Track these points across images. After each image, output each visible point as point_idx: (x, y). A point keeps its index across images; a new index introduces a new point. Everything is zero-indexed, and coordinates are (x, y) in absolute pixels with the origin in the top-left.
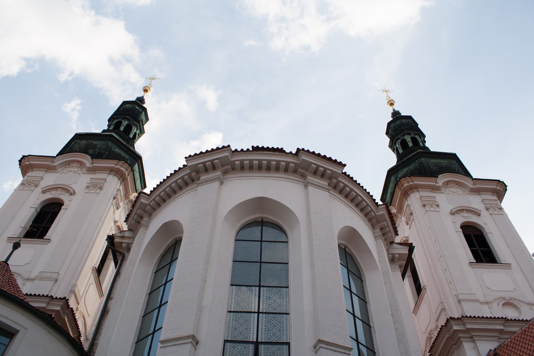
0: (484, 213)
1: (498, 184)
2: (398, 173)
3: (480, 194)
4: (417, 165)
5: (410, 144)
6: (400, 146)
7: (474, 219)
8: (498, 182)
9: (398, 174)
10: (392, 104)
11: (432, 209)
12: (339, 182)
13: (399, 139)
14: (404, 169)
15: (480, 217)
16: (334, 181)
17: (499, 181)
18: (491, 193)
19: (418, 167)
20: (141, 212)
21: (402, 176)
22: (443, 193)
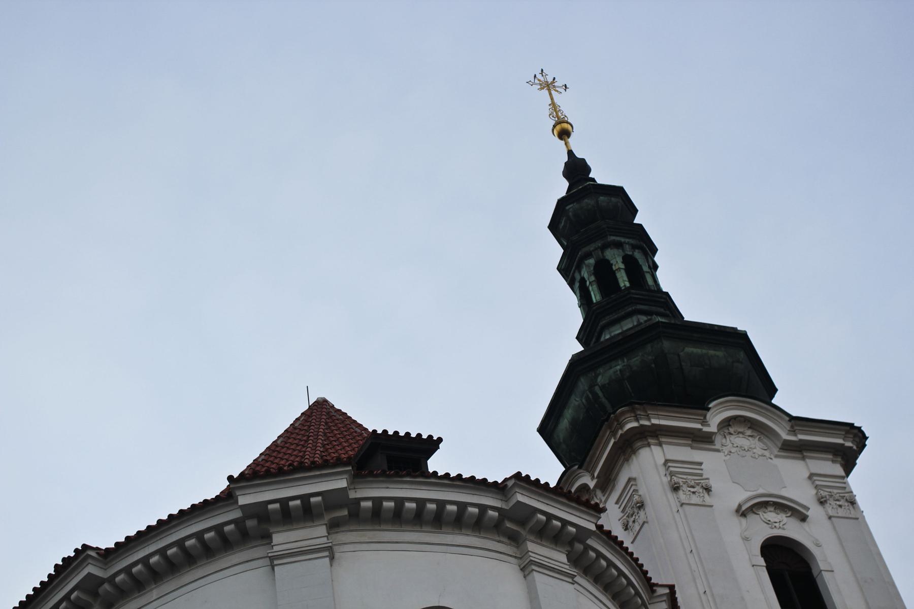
0: (815, 512)
1: (847, 432)
2: (598, 372)
3: (803, 458)
4: (650, 357)
5: (623, 281)
6: (593, 278)
7: (791, 529)
8: (848, 428)
9: (596, 377)
10: (564, 134)
11: (695, 499)
12: (588, 548)
13: (588, 255)
15: (805, 525)
16: (579, 547)
17: (851, 426)
18: (831, 457)
19: (653, 366)
20: (83, 596)
21: (607, 381)
22: (718, 451)
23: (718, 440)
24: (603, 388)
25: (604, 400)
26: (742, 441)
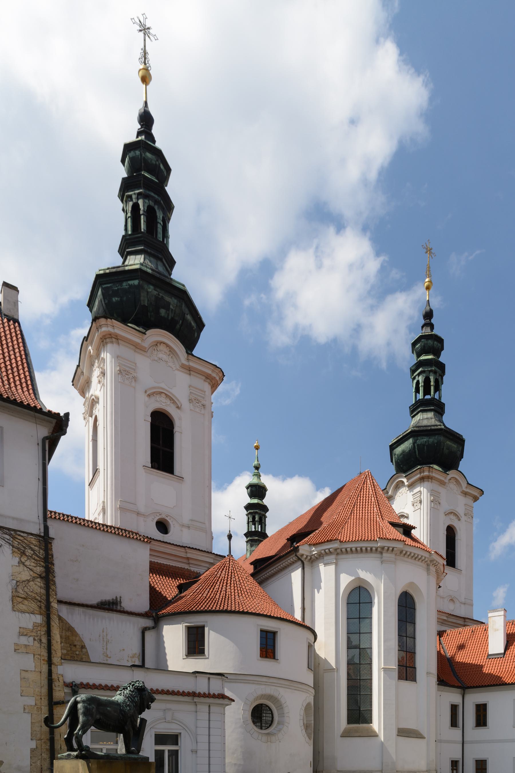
0: (463, 518)
3: (465, 496)
9: (417, 439)
14: (424, 437)
15: (459, 521)
23: (447, 484)
24: (418, 445)
25: (416, 450)
26: (452, 486)
